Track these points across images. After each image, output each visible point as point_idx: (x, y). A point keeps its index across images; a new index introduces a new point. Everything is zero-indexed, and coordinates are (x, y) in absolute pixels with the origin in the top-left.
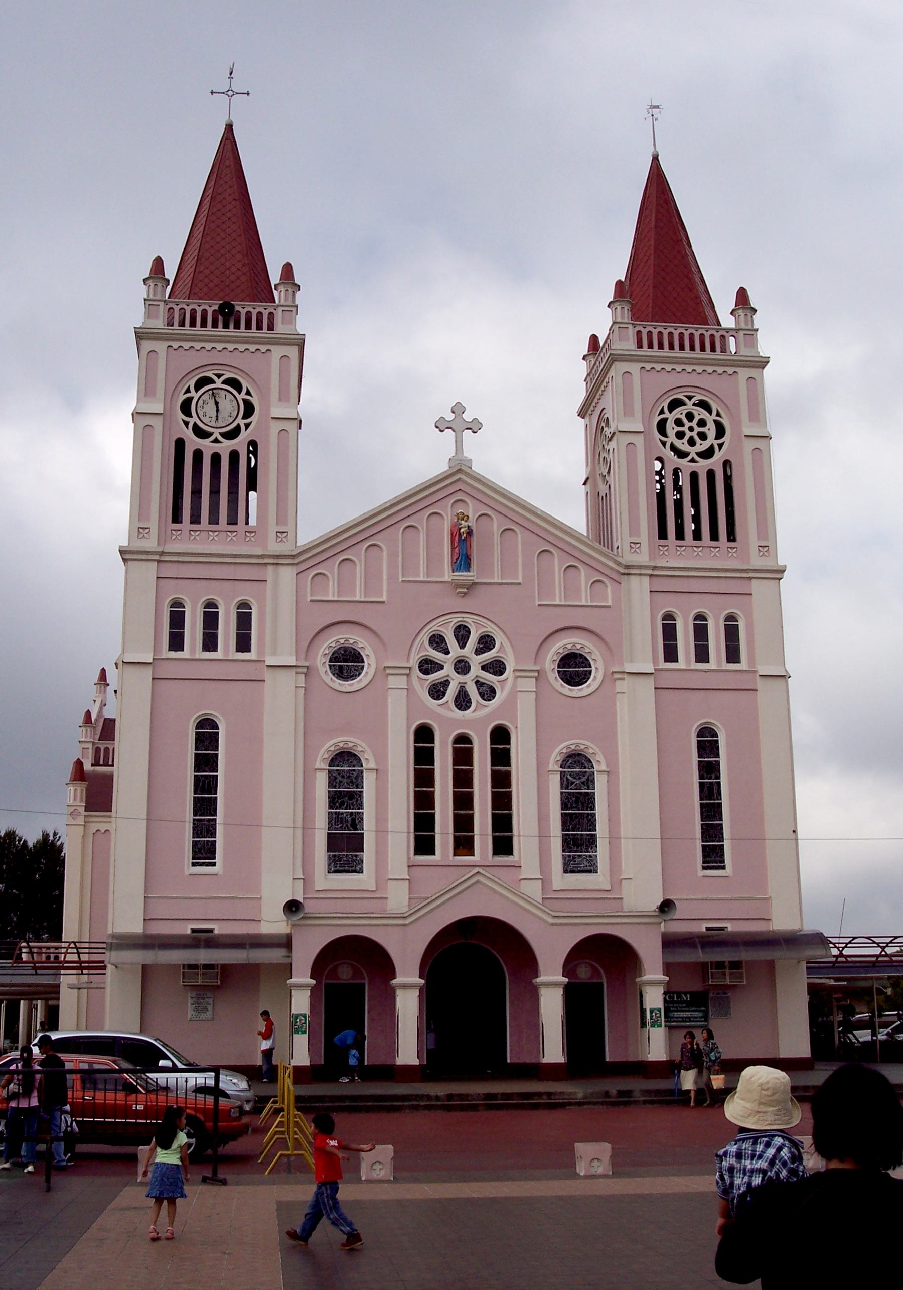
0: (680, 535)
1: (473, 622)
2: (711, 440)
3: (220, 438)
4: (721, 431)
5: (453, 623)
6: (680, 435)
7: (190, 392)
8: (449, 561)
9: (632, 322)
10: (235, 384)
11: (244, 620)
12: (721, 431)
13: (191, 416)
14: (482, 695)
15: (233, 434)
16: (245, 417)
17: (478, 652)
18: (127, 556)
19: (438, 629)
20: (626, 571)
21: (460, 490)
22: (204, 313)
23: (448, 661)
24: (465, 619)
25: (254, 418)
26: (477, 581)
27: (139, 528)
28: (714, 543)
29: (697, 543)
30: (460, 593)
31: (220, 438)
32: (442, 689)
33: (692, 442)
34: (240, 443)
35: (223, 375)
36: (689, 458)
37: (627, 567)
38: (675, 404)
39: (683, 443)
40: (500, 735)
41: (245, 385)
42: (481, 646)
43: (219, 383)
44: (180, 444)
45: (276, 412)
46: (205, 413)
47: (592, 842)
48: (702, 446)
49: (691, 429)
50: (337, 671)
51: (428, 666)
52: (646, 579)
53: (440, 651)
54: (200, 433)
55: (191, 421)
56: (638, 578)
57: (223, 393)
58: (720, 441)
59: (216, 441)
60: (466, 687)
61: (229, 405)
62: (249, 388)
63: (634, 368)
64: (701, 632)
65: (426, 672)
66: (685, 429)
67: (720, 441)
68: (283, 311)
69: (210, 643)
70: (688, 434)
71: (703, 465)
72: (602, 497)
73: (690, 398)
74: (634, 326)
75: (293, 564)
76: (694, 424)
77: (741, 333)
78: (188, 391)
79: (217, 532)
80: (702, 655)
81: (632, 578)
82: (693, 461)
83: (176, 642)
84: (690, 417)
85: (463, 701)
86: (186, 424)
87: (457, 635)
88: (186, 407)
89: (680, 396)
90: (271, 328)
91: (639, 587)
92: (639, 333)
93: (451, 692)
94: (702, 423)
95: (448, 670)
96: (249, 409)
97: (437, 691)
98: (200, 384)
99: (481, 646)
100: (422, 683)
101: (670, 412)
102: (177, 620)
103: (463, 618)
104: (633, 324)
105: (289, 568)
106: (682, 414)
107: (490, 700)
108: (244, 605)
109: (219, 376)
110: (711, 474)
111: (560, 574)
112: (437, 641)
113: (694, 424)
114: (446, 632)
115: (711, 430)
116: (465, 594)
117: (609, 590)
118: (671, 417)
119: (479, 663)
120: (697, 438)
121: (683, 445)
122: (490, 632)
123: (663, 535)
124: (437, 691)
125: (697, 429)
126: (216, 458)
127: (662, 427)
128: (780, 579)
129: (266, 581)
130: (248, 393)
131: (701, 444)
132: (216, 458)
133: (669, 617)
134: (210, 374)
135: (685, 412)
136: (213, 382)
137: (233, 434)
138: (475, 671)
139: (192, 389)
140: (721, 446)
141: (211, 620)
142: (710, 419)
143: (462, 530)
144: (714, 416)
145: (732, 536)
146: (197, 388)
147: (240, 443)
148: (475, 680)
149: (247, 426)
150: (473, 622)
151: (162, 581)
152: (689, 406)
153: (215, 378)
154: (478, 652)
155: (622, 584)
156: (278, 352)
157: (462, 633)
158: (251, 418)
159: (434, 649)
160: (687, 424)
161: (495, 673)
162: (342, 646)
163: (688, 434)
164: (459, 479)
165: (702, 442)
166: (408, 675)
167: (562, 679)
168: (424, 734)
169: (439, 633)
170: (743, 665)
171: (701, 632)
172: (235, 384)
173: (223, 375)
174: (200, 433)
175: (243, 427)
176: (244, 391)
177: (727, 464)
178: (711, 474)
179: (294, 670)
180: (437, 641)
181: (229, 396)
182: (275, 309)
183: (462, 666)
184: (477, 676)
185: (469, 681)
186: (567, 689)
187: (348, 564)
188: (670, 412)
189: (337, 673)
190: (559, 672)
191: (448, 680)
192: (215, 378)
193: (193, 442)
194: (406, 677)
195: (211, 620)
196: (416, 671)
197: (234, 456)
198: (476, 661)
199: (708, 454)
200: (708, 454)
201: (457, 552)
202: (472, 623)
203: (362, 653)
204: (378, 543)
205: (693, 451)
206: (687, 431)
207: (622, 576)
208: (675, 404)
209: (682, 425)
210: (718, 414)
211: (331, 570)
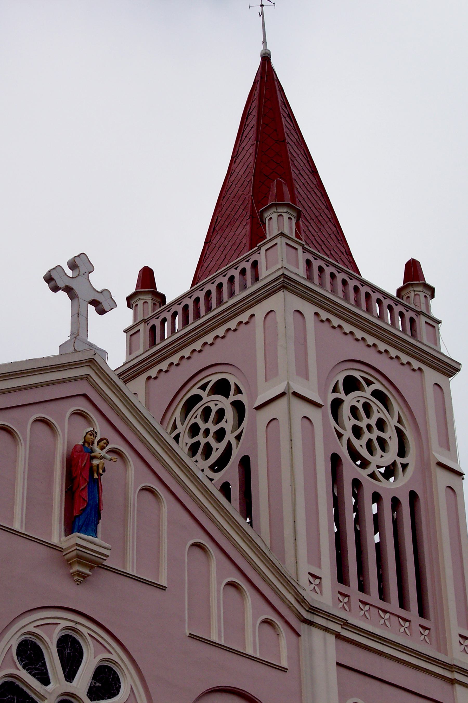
1: (89, 635)
5: (59, 627)
19: (37, 631)
21: (85, 396)
24: (79, 627)
30: (79, 574)
37: (313, 610)
42: (98, 684)
52: (331, 639)
73: (369, 383)
77: (423, 319)
94: (381, 425)
99: (98, 684)
101: (347, 394)
103: (76, 623)
104: (303, 248)
106: (358, 401)
111: (218, 591)
116: (84, 576)
117: (283, 642)
125: (376, 433)
131: (382, 456)
135: (362, 401)
143: (95, 462)
150: (89, 635)
155: (302, 637)
164: (86, 378)
165: (383, 454)
188: (347, 394)
206: (365, 429)
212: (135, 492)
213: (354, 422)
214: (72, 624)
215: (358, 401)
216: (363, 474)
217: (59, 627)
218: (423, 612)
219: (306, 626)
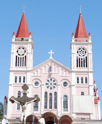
0: (80, 66)
4: (86, 52)
11: (24, 79)
12: (86, 52)
15: (23, 55)
17: (53, 82)
22: (20, 39)
28: (84, 68)
34: (24, 56)
38: (79, 49)
40: (56, 93)
44: (17, 56)
46: (19, 53)
47: (67, 107)
48: (83, 54)
51: (47, 84)
54: (19, 55)
61: (23, 50)
64: (82, 79)
65: (46, 85)
69: (20, 81)
71: (83, 57)
76: (82, 52)
80: (82, 82)
83: (16, 82)
85: (51, 88)
88: (17, 52)
90: (28, 41)
91: (73, 74)
92: (75, 40)
93: (50, 87)
95: (49, 85)
96: (25, 51)
97: (48, 88)
98: (19, 48)
100: (46, 86)
102: (16, 78)
113: (82, 52)
118: (79, 51)
123: (77, 66)
124: (48, 88)
126: (21, 58)
127: (78, 52)
132: (21, 58)
133: (78, 77)
137: (23, 55)
141: (20, 79)
142: (84, 51)
144: (85, 50)
145: (87, 66)
146: (19, 49)
152: (82, 49)
157: (51, 79)
168: (46, 93)
171: (82, 79)
172: (23, 48)
174: (19, 55)
177: (86, 57)
183: (51, 84)
186: (64, 87)
193: (18, 56)
197: (23, 58)
208: (79, 49)
218: (87, 66)
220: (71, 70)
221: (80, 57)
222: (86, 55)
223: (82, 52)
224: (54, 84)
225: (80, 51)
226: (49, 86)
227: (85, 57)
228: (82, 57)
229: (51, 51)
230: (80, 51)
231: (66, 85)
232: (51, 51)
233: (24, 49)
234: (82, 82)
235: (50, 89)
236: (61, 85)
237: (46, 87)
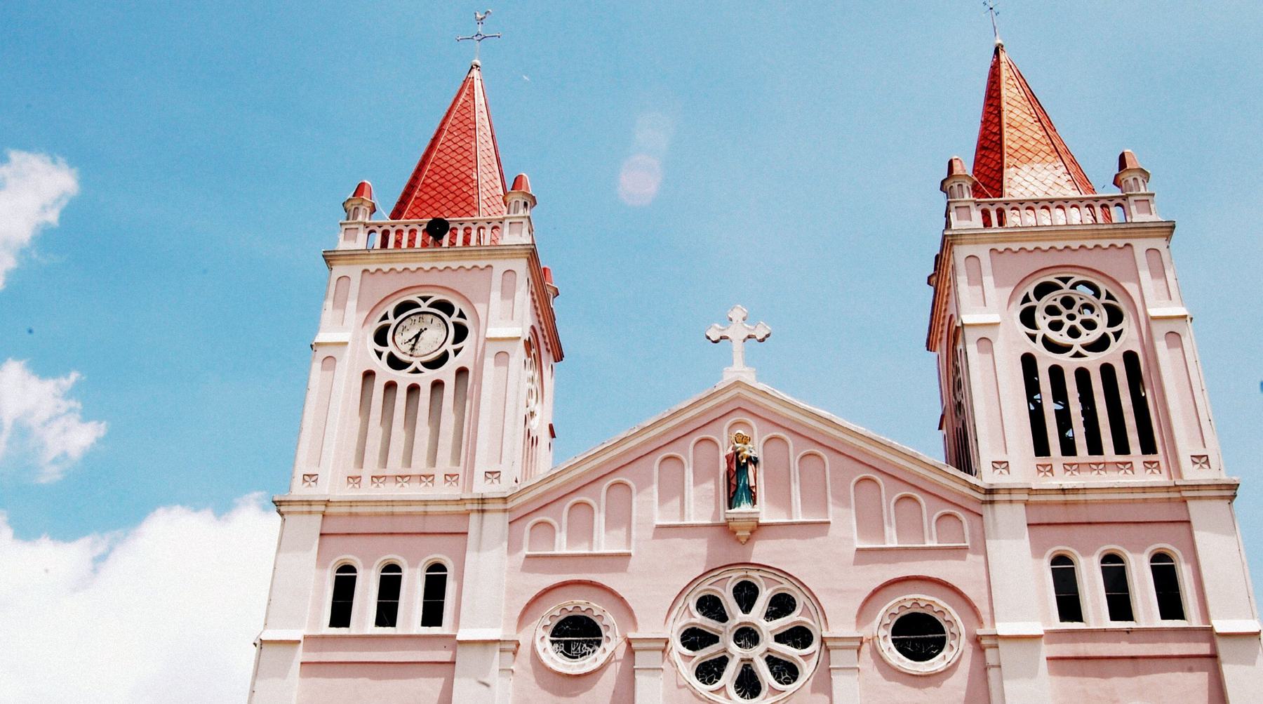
2: (1102, 327)
3: (421, 368)
6: (1056, 326)
7: (388, 319)
8: (724, 500)
9: (975, 199)
10: (447, 307)
12: (1115, 316)
13: (386, 345)
14: (777, 676)
16: (456, 341)
17: (771, 615)
18: (283, 509)
19: (710, 587)
20: (988, 498)
21: (739, 408)
23: (726, 632)
24: (749, 573)
25: (466, 344)
26: (763, 520)
27: (304, 475)
29: (1096, 458)
31: (421, 368)
32: (715, 669)
33: (1074, 333)
35: (430, 297)
36: (1073, 352)
37: (990, 491)
38: (1042, 290)
39: (1061, 335)
41: (458, 305)
42: (774, 609)
43: (424, 307)
45: (492, 332)
49: (1072, 317)
50: (563, 649)
51: (694, 639)
53: (713, 618)
54: (395, 363)
55: (386, 351)
56: (1008, 506)
57: (429, 317)
58: (1117, 329)
59: (417, 371)
60: (752, 665)
62: (463, 311)
63: (983, 251)
66: (1063, 318)
67: (1117, 329)
68: (510, 223)
70: (1068, 324)
71: (1093, 361)
72: (960, 429)
74: (978, 204)
75: (505, 511)
76: (1074, 311)
78: (385, 317)
79: (408, 478)
80: (1120, 606)
81: (997, 507)
82: (1078, 355)
84: (1068, 302)
86: (379, 354)
87: (739, 595)
88: (381, 337)
89: (1051, 279)
98: (402, 308)
99: (774, 609)
100: (684, 663)
105: (501, 515)
106: (1055, 300)
107: (788, 683)
108: (438, 567)
109: (425, 299)
110: (1107, 370)
111: (888, 507)
112: (710, 606)
114: (722, 591)
115: (1102, 319)
119: (771, 632)
120: (1081, 328)
121: (1061, 337)
122: (788, 589)
123: (1041, 448)
127: (1028, 318)
128: (1235, 496)
129: (467, 533)
130: (461, 315)
131: (1088, 335)
134: (414, 298)
135: (1059, 298)
136: (418, 306)
138: (768, 642)
139: (391, 315)
140: (1117, 335)
145: (1148, 446)
147: (446, 373)
148: (766, 655)
149: (457, 352)
150: (761, 576)
151: (327, 539)
153: (420, 302)
154: (771, 615)
156: (500, 266)
157: (746, 594)
158: (463, 342)
159: (704, 615)
160: (1065, 312)
161: (796, 645)
162: (571, 614)
163: (1068, 324)
165: (1088, 332)
166: (664, 651)
167: (900, 650)
169: (712, 593)
170: (1193, 618)
173: (430, 297)
174: (395, 363)
175: (451, 353)
176: (456, 312)
178: (1107, 370)
179: (498, 646)
180: (710, 606)
181: (437, 320)
182: (501, 223)
183: (747, 636)
184: (768, 651)
185: (757, 655)
187: (582, 509)
189: (562, 652)
190: (894, 641)
191: (724, 657)
192: (420, 302)
194: (660, 653)
195: (390, 586)
196: (677, 646)
198: (768, 629)
199: (1101, 345)
200: (1101, 345)
201: (735, 483)
202: (761, 579)
203: (599, 623)
204: (629, 482)
205: (1077, 344)
207: (983, 506)
208: (1042, 290)
209: (1059, 313)
210: (1109, 296)
211: (560, 516)
212: (794, 461)
213: (1050, 318)
214: (744, 573)
215: (1055, 300)
216: (1063, 360)
217: (731, 580)
219: (988, 506)
220: (972, 479)
221: (1063, 360)
222: (1130, 339)
223: (1077, 323)
224: (779, 638)
225: (1051, 310)
226: (722, 662)
227: (1113, 356)
228: (1079, 362)
229: (737, 314)
230: (1051, 310)
231: (940, 644)
232: (737, 314)
233: (450, 313)
234: (1120, 606)
235: (732, 691)
236: (866, 648)
237: (688, 672)
